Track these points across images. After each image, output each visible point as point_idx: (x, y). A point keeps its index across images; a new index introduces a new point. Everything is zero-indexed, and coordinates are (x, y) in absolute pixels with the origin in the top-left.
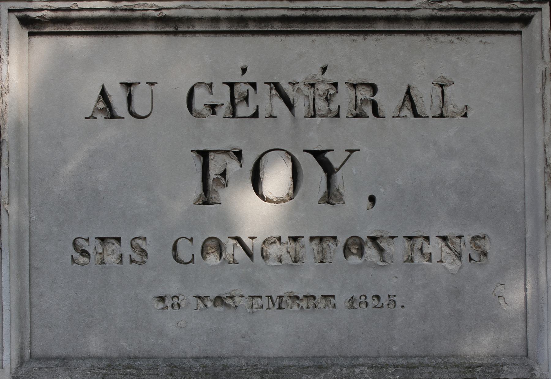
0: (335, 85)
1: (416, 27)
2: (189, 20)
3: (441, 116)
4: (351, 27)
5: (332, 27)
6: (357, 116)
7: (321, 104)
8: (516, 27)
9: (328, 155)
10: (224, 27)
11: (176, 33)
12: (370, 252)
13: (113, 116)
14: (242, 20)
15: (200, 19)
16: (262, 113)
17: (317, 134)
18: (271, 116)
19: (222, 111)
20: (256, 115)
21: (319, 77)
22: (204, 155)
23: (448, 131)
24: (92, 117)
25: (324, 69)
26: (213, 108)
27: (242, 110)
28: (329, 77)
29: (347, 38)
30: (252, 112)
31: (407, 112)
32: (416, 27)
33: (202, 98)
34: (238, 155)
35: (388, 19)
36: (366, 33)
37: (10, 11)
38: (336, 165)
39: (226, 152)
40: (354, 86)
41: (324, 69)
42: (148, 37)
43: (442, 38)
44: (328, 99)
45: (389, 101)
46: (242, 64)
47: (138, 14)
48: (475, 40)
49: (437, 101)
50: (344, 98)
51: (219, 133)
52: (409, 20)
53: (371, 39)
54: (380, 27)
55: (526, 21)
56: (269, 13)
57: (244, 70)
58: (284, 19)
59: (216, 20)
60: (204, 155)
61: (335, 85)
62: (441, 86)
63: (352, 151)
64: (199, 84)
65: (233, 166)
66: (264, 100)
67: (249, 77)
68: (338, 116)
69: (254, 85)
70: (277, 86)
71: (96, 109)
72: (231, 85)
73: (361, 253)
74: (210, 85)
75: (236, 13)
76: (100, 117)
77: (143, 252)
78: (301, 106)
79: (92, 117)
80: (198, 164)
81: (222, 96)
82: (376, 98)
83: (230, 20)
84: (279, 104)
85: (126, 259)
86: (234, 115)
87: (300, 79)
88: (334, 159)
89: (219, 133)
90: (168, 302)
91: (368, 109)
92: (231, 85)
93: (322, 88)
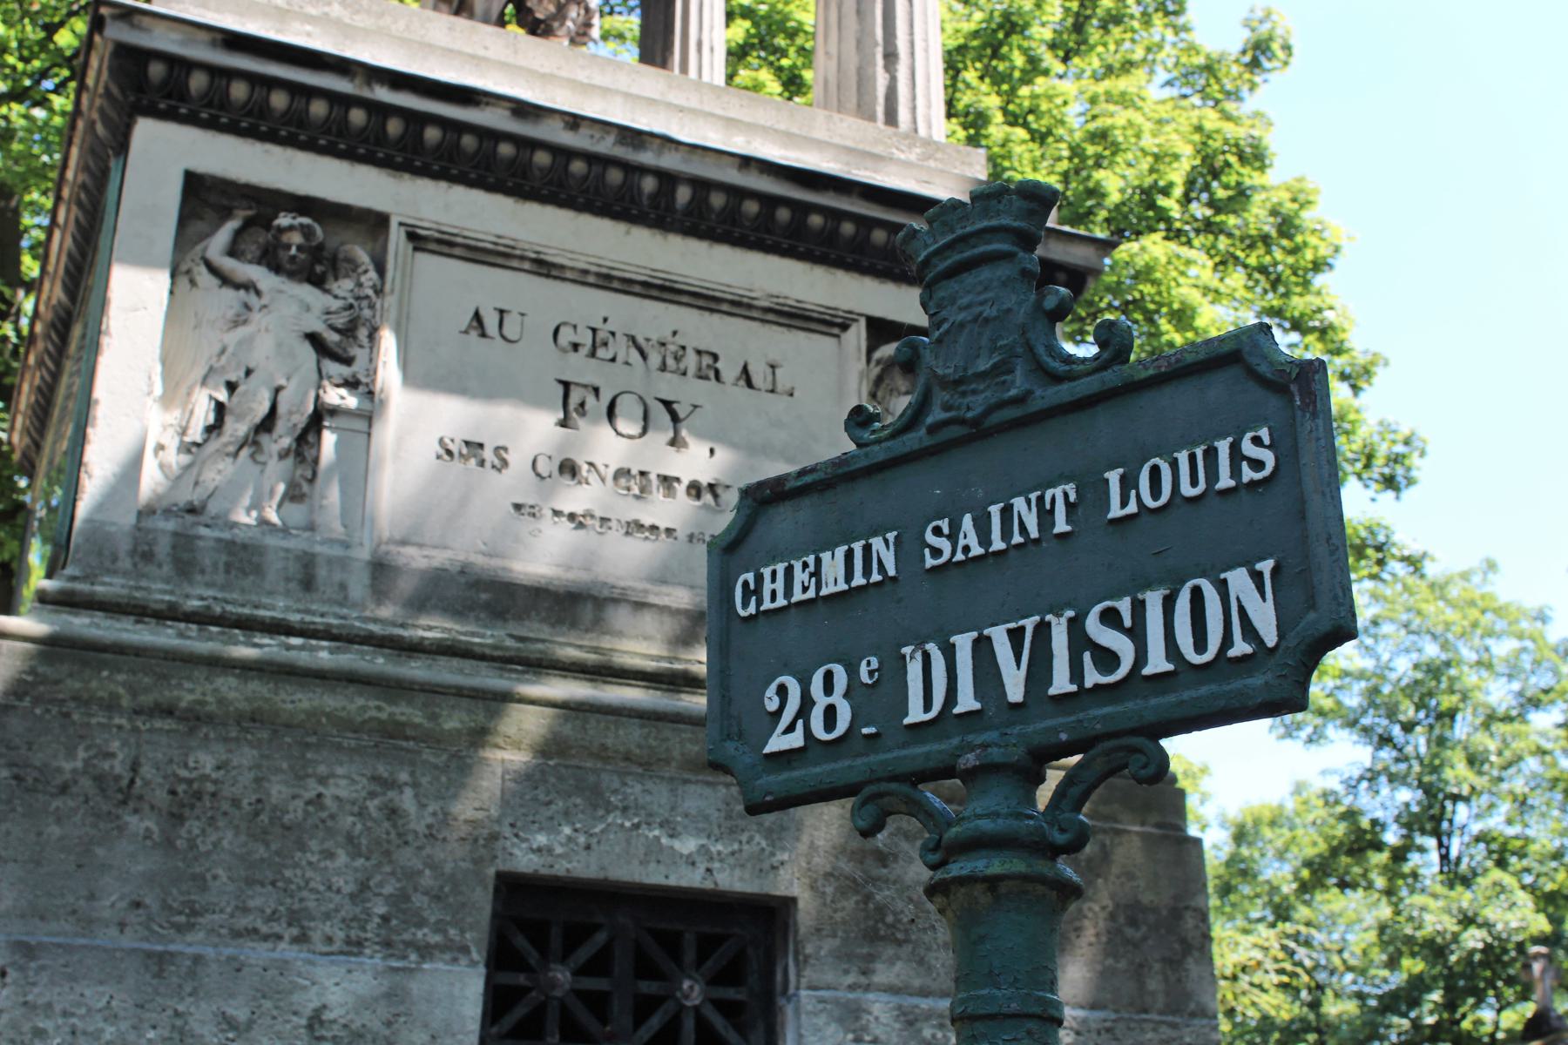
0: (683, 348)
1: (755, 314)
2: (562, 267)
3: (772, 391)
4: (701, 303)
5: (685, 299)
6: (700, 377)
7: (670, 362)
8: (836, 331)
9: (675, 406)
10: (591, 279)
11: (548, 276)
12: (708, 498)
13: (483, 335)
14: (608, 277)
15: (572, 269)
16: (620, 359)
17: (668, 386)
18: (627, 363)
19: (584, 351)
20: (613, 360)
21: (670, 338)
22: (566, 385)
23: (779, 404)
24: (466, 332)
25: (675, 333)
26: (576, 347)
27: (601, 352)
28: (680, 340)
29: (695, 312)
30: (610, 356)
31: (742, 383)
32: (755, 314)
33: (566, 336)
34: (596, 391)
35: (733, 303)
36: (712, 311)
37: (401, 224)
38: (682, 415)
39: (585, 386)
40: (699, 352)
41: (675, 333)
42: (522, 275)
43: (775, 328)
44: (677, 359)
45: (730, 371)
46: (604, 314)
47: (518, 252)
48: (802, 335)
49: (770, 378)
50: (691, 360)
51: (580, 369)
52: (750, 307)
53: (716, 317)
54: (725, 307)
55: (844, 327)
56: (634, 277)
57: (605, 320)
58: (645, 284)
59: (585, 272)
60: (566, 385)
61: (683, 348)
62: (773, 367)
63: (695, 407)
64: (565, 324)
65: (591, 400)
66: (620, 347)
67: (610, 326)
68: (684, 374)
69: (613, 334)
70: (633, 339)
71: (470, 326)
72: (594, 330)
73: (698, 496)
74: (575, 327)
75: (604, 271)
76: (474, 334)
77: (505, 463)
78: (655, 359)
79: (466, 332)
80: (560, 389)
81: (586, 339)
82: (719, 365)
83: (598, 275)
84: (635, 356)
85: (488, 465)
86: (593, 354)
87: (655, 337)
88: (682, 410)
89: (580, 369)
90: (526, 510)
91: (712, 374)
92: (594, 330)
93: (672, 348)
